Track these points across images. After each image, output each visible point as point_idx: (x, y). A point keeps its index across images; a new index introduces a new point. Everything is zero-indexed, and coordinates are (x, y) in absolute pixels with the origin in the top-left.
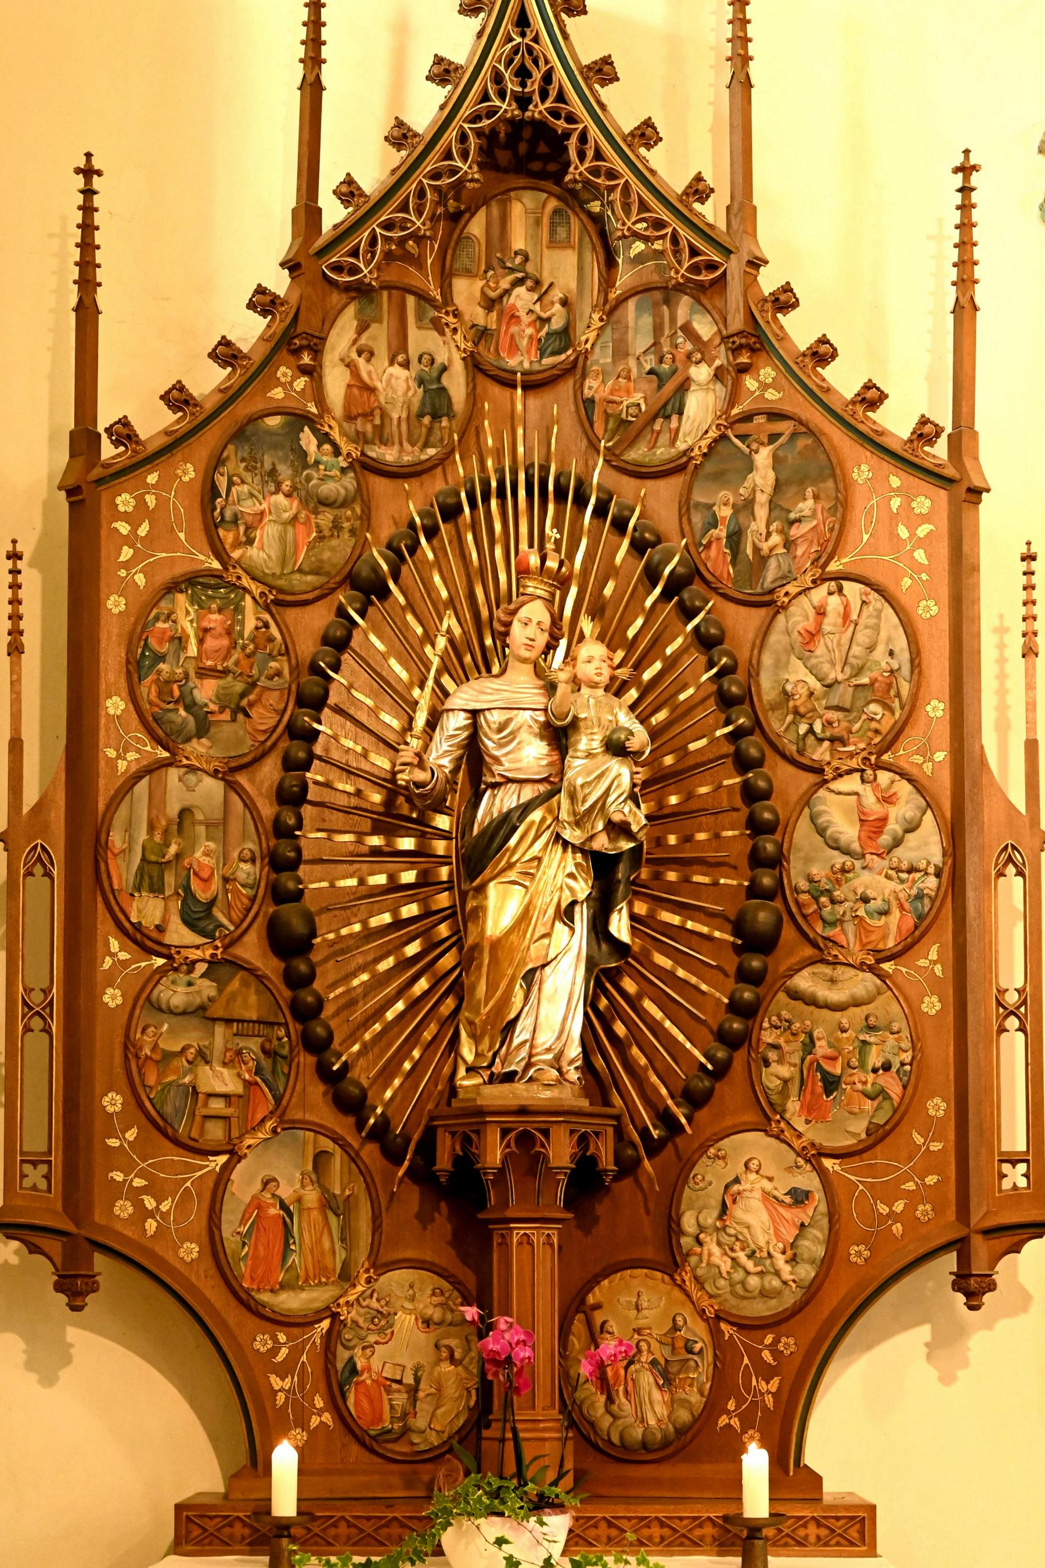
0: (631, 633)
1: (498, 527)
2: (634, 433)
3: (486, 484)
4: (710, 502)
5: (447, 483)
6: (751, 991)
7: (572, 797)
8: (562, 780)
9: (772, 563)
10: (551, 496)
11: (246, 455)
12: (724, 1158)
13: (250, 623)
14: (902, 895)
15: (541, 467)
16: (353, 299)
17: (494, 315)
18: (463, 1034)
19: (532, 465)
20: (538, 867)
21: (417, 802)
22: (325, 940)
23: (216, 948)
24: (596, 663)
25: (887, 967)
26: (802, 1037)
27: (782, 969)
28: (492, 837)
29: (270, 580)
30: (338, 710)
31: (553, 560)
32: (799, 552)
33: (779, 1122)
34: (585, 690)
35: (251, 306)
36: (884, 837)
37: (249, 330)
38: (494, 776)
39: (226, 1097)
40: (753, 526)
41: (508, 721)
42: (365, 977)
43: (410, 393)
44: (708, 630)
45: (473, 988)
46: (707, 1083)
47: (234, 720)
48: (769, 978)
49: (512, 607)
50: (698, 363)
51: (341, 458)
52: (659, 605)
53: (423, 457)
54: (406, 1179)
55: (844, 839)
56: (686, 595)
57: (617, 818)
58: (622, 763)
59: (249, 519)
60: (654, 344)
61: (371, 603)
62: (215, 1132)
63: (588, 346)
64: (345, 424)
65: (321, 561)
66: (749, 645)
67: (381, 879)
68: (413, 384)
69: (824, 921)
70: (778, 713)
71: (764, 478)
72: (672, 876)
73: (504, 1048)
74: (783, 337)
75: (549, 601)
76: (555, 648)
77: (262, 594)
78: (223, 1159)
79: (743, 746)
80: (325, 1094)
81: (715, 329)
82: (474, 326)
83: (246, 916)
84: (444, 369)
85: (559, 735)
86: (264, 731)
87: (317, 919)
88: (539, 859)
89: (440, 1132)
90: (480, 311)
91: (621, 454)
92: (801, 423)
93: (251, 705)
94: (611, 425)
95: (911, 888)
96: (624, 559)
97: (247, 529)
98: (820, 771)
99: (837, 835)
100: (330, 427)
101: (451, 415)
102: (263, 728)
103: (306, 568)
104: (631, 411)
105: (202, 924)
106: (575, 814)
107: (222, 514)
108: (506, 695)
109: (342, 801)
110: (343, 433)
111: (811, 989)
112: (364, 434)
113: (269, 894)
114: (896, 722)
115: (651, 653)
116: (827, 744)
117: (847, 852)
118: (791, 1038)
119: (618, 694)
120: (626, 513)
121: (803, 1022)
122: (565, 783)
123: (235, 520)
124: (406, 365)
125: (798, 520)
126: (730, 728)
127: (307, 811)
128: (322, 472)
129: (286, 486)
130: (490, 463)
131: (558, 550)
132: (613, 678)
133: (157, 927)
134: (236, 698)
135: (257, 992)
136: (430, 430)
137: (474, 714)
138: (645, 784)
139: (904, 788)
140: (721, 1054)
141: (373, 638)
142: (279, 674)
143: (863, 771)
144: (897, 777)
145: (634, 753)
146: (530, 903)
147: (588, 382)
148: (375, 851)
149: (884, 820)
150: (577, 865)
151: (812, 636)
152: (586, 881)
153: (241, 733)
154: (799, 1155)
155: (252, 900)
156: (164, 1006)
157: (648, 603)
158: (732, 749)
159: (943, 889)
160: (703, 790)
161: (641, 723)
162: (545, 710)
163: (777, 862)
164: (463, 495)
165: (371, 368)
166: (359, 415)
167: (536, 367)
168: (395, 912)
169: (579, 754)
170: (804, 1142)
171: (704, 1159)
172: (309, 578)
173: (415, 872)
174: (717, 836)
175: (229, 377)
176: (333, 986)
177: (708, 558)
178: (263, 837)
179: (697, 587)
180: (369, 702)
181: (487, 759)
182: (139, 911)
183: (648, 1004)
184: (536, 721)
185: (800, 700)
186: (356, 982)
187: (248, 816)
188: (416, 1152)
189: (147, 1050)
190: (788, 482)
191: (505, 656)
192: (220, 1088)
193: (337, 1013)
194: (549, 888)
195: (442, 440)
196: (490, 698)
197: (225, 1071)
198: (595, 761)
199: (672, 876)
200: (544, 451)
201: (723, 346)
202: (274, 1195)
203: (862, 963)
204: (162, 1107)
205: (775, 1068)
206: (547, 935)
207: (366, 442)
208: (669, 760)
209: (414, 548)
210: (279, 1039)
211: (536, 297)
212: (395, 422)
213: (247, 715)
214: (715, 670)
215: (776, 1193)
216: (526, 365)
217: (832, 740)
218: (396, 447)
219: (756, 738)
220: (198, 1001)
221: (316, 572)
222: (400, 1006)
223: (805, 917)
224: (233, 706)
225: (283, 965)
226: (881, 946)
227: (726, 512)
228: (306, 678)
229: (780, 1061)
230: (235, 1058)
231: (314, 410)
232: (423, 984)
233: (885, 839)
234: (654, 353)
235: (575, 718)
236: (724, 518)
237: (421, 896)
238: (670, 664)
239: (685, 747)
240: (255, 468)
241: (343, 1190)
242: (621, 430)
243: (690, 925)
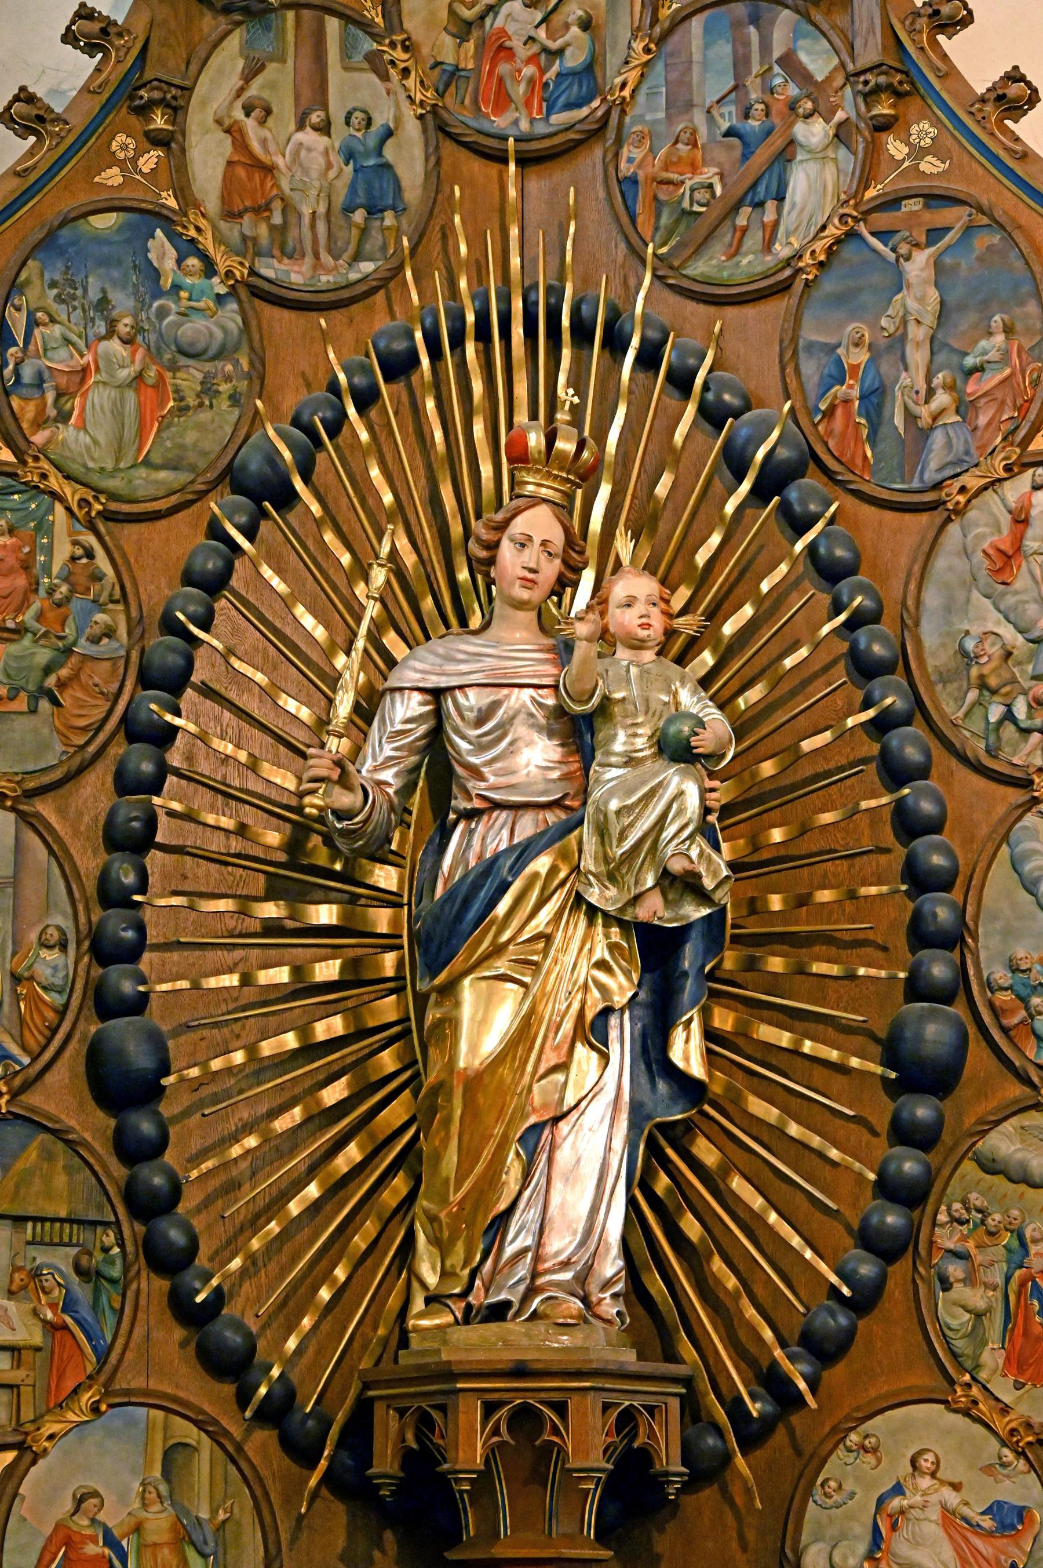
0: (701, 558)
1: (478, 387)
2: (703, 232)
3: (457, 318)
4: (832, 340)
5: (393, 317)
6: (918, 1160)
7: (602, 832)
8: (584, 803)
9: (938, 438)
10: (566, 336)
11: (57, 277)
12: (875, 1450)
13: (63, 551)
15: (549, 290)
16: (238, 24)
17: (470, 46)
18: (421, 1238)
19: (535, 286)
20: (545, 952)
21: (339, 842)
22: (182, 1080)
24: (640, 608)
26: (1006, 1238)
27: (969, 1122)
28: (467, 903)
29: (95, 479)
30: (207, 691)
31: (568, 439)
32: (982, 420)
33: (969, 1386)
34: (623, 654)
35: (69, 37)
37: (66, 75)
38: (470, 799)
40: (905, 379)
41: (495, 705)
42: (252, 1142)
43: (332, 174)
44: (830, 551)
45: (437, 1158)
46: (843, 1321)
47: (33, 711)
48: (946, 1137)
49: (500, 516)
50: (808, 116)
51: (216, 280)
52: (749, 512)
53: (354, 276)
54: (324, 1492)
56: (793, 494)
57: (677, 866)
58: (685, 774)
59: (63, 381)
60: (735, 88)
61: (265, 514)
63: (626, 93)
64: (223, 225)
65: (182, 447)
66: (903, 576)
67: (282, 975)
68: (337, 160)
70: (952, 687)
71: (921, 300)
72: (776, 964)
73: (489, 1262)
74: (950, 73)
75: (563, 508)
76: (575, 585)
77: (83, 502)
79: (894, 743)
80: (184, 1344)
81: (836, 61)
82: (437, 64)
83: (50, 1040)
84: (389, 133)
85: (579, 730)
86: (84, 729)
87: (171, 1044)
88: (547, 938)
89: (379, 1409)
90: (448, 41)
91: (683, 265)
92: (980, 210)
93: (62, 685)
94: (664, 220)
96: (687, 437)
97: (59, 395)
98: (1026, 784)
100: (198, 229)
101: (399, 210)
102: (82, 723)
103: (156, 458)
104: (697, 196)
106: (606, 860)
107: (17, 372)
108: (489, 662)
109: (216, 844)
110: (219, 239)
111: (1019, 1156)
112: (255, 240)
113: (90, 1003)
115: (739, 591)
118: (986, 1240)
119: (681, 660)
120: (692, 362)
121: (1006, 1213)
122: (590, 809)
123: (39, 382)
124: (325, 128)
125: (979, 369)
126: (871, 713)
127: (154, 859)
128: (185, 303)
129: (124, 327)
130: (463, 284)
131: (577, 421)
132: (670, 634)
134: (36, 675)
136: (364, 232)
137: (437, 694)
138: (726, 811)
140: (867, 1269)
141: (267, 572)
142: (109, 633)
145: (707, 757)
146: (532, 1011)
147: (625, 152)
148: (272, 928)
150: (612, 947)
151: (1006, 560)
152: (627, 974)
153: (46, 731)
154: (1004, 1444)
155: (62, 1012)
157: (730, 508)
158: (874, 749)
160: (827, 818)
161: (721, 707)
162: (555, 687)
163: (954, 939)
164: (418, 335)
165: (266, 133)
166: (246, 210)
167: (541, 129)
168: (304, 1031)
169: (613, 759)
170: (1012, 1421)
171: (841, 1451)
172: (162, 475)
173: (338, 962)
174: (852, 895)
175: (31, 152)
176: (196, 1159)
177: (830, 433)
178: (81, 907)
179: (811, 481)
180: (259, 677)
181: (459, 770)
183: (737, 1183)
184: (540, 705)
185: (988, 666)
186: (236, 1151)
187: (56, 871)
188: (340, 1445)
190: (962, 308)
191: (490, 600)
193: (206, 1204)
194: (564, 987)
195: (384, 248)
196: (464, 668)
197: (11, 1305)
198: (640, 771)
199: (776, 964)
200: (555, 263)
201: (848, 90)
202: (93, 1521)
205: (959, 1291)
206: (563, 1067)
207: (258, 254)
208: (768, 768)
209: (336, 425)
210: (106, 1250)
211: (539, 16)
212: (306, 220)
213: (55, 702)
214: (842, 617)
215: (966, 1511)
216: (524, 125)
218: (309, 259)
219: (917, 729)
221: (173, 466)
222: (313, 1191)
223: (1005, 1030)
224: (31, 687)
225: (113, 1123)
227: (860, 357)
228: (156, 640)
229: (970, 1280)
231: (172, 203)
232: (353, 1153)
234: (736, 102)
235: (606, 699)
236: (855, 368)
237: (350, 1004)
238: (770, 607)
239: (796, 746)
240: (74, 298)
241: (214, 1512)
242: (682, 228)
243: (807, 1046)
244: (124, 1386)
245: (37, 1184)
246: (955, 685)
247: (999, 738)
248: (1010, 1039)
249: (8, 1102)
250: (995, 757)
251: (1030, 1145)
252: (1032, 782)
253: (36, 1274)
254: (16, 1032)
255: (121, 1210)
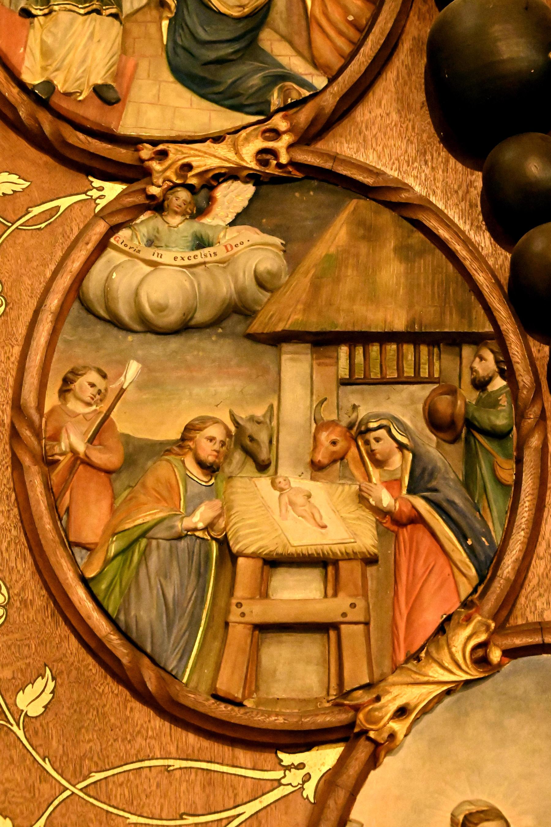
23: (276, 134)
39: (321, 562)
62: (295, 677)
78: (323, 759)
83: (357, 47)
105: (229, 76)
133: (99, 91)
135: (405, 252)
156: (124, 311)
182: (47, 53)
189: (75, 440)
192: (302, 538)
197: (319, 490)
204: (125, 606)
210: (481, 385)
220: (225, 288)
230: (345, 450)
244: (532, 618)
245: (350, 280)
249: (290, 147)
253: (359, 432)
254: (300, 41)
255: (502, 312)
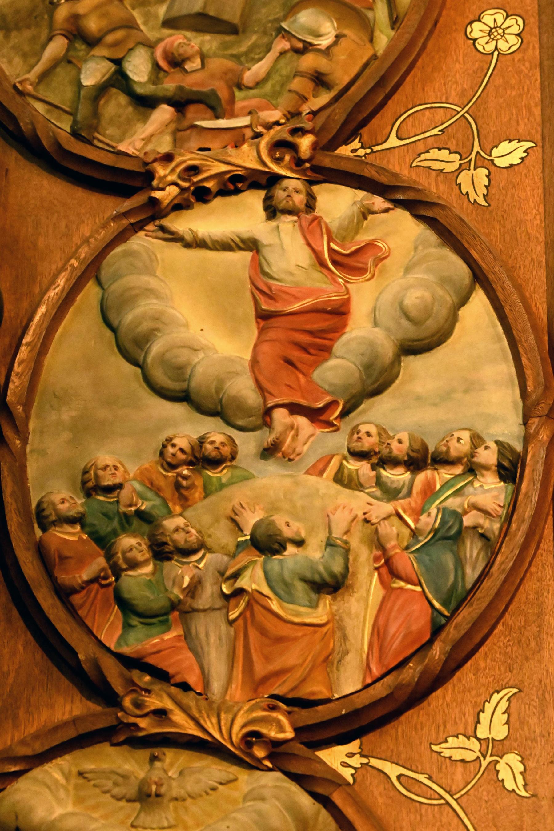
14: (391, 530)
25: (337, 758)
36: (332, 362)
55: (202, 373)
69: (126, 606)
95: (418, 513)
99: (183, 356)
114: (374, 57)
116: (164, 113)
117: (215, 408)
139: (401, 232)
143: (274, 180)
144: (379, 202)
149: (339, 312)
159: (526, 511)
203: (252, 738)
217: (181, 103)
223: (64, 594)
226: (316, 689)
233: (337, 370)
246: (27, 34)
247: (96, 114)
248: (72, 611)
250: (89, 142)
251: (95, 808)
252: (150, 175)
